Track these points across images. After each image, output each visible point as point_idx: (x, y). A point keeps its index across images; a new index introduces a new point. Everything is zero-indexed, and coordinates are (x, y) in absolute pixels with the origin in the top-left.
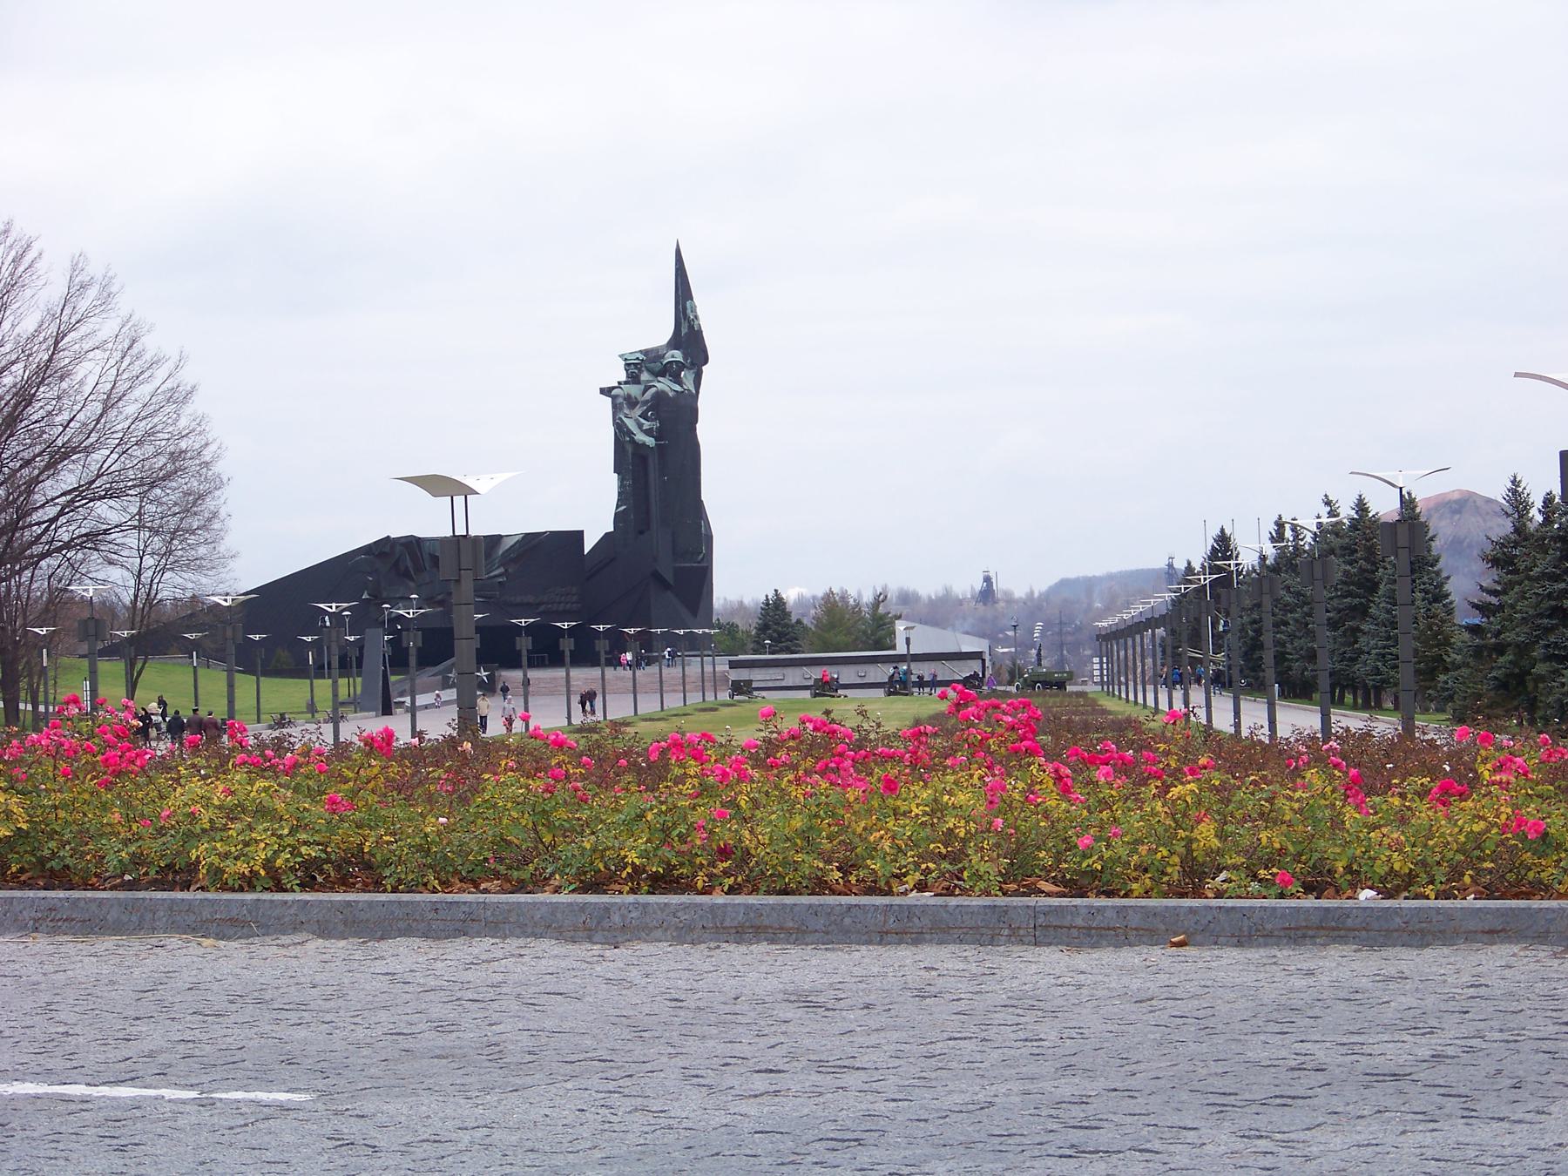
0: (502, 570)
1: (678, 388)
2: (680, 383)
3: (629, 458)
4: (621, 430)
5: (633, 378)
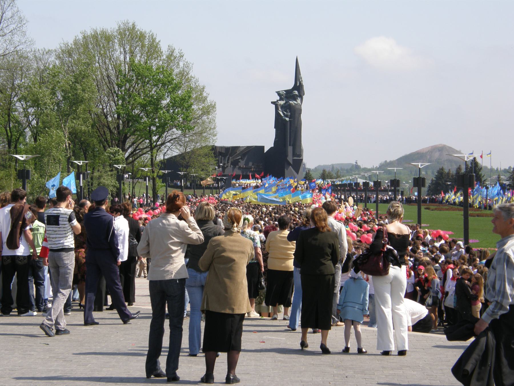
0: (240, 157)
1: (296, 102)
2: (296, 101)
3: (279, 123)
4: (277, 115)
5: (281, 99)
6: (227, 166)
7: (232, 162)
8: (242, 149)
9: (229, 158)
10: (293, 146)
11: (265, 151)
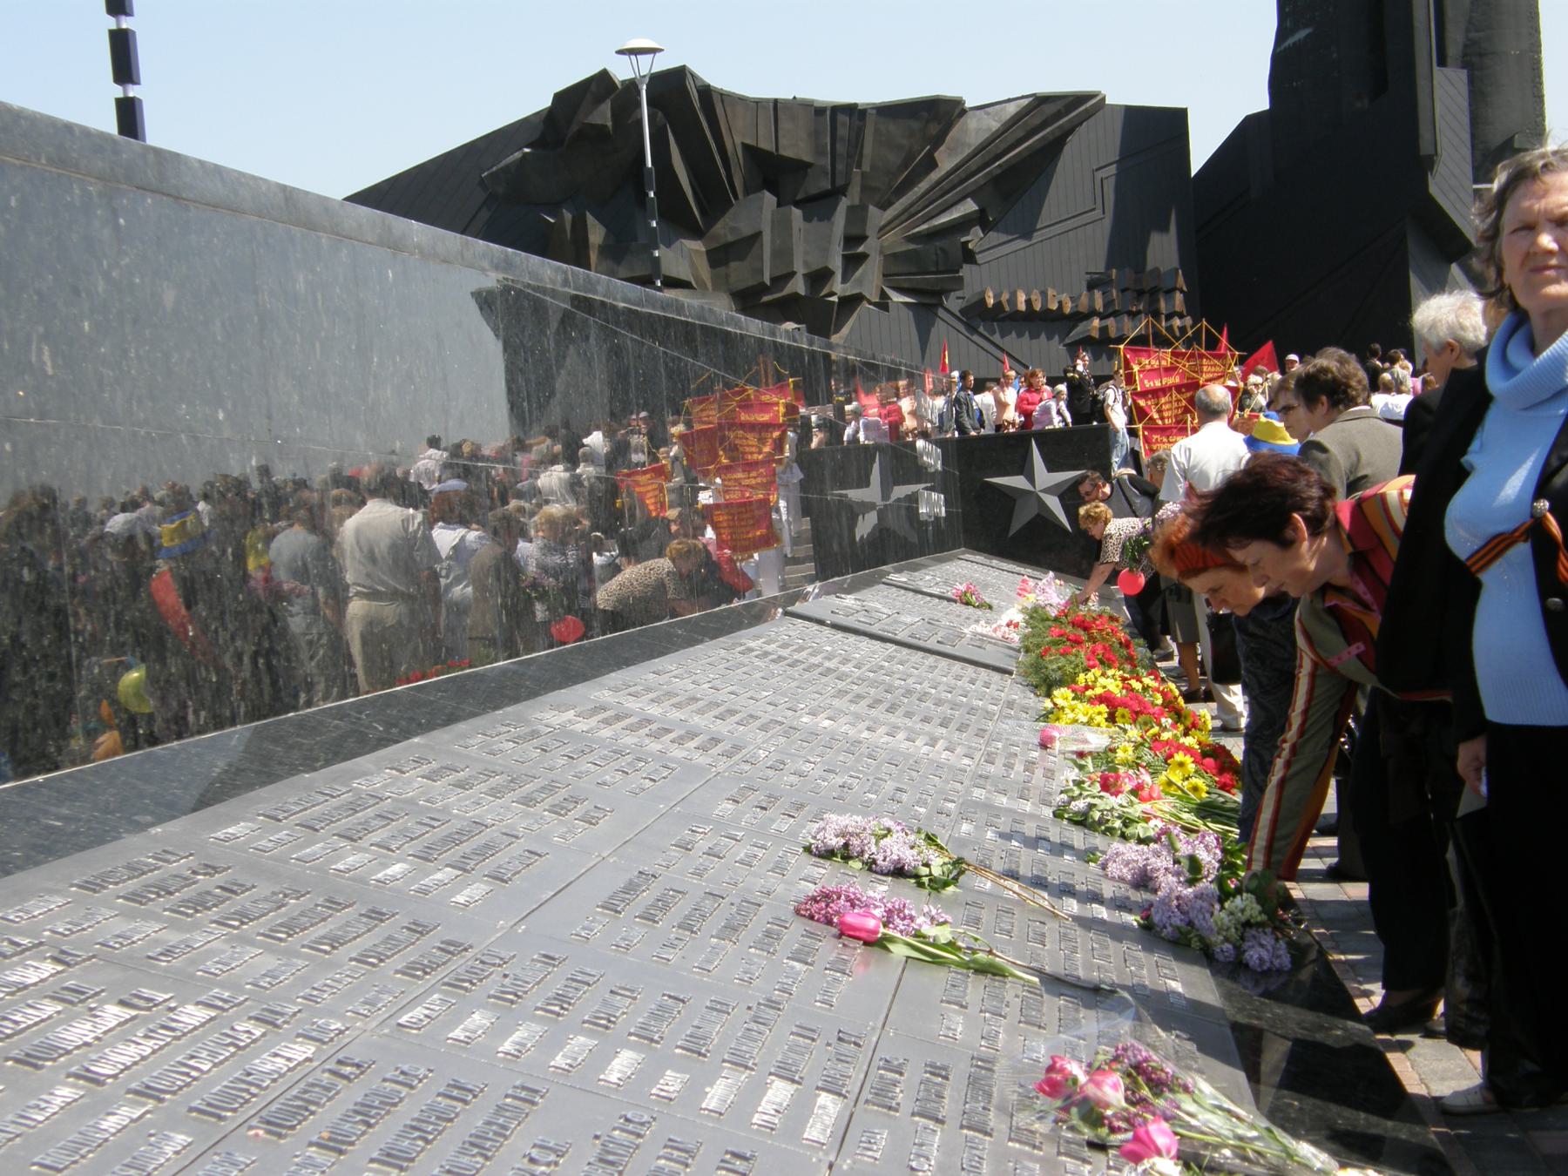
0: (970, 206)
6: (851, 303)
7: (892, 258)
8: (973, 132)
9: (857, 214)
10: (1466, 65)
11: (1198, 161)
